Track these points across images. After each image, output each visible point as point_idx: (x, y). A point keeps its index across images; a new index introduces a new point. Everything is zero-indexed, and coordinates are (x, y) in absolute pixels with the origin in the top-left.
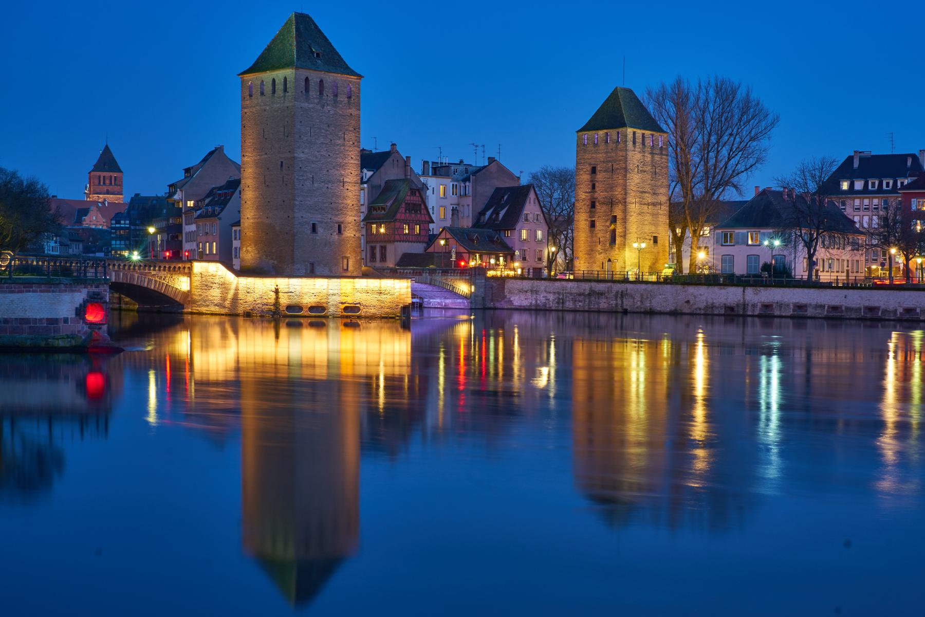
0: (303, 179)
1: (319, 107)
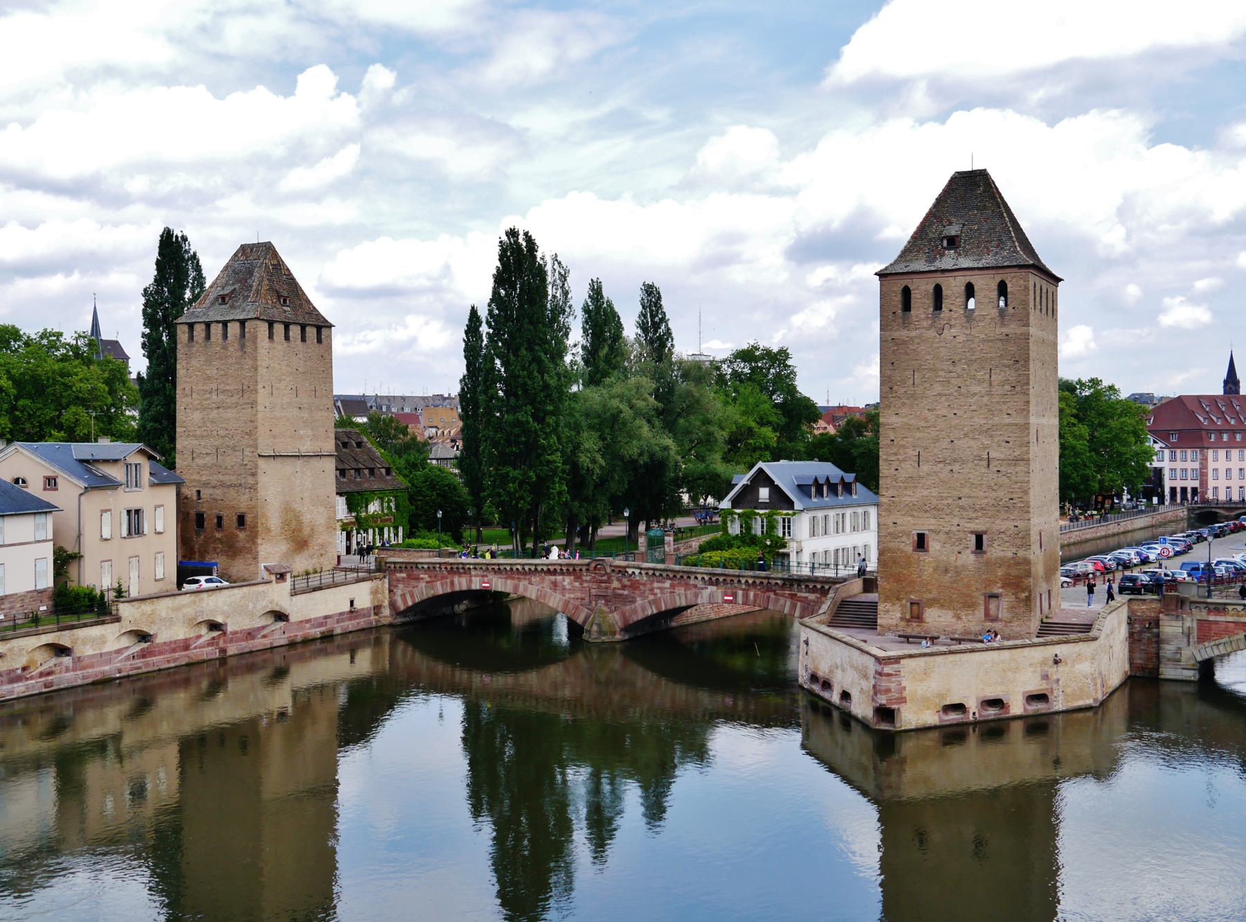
0: (898, 460)
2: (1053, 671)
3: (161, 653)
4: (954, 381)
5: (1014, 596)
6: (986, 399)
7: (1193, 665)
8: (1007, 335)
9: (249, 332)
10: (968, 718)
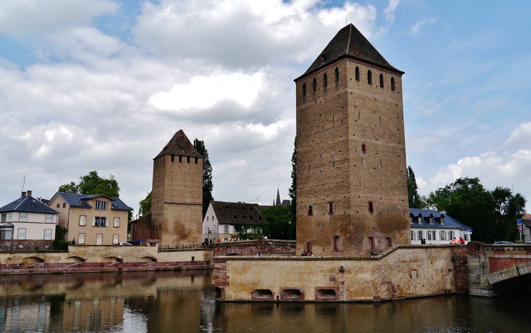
0: (302, 169)
1: (313, 103)
2: (340, 277)
3: (88, 266)
4: (321, 125)
5: (344, 237)
6: (332, 130)
7: (487, 286)
8: (339, 95)
10: (274, 299)
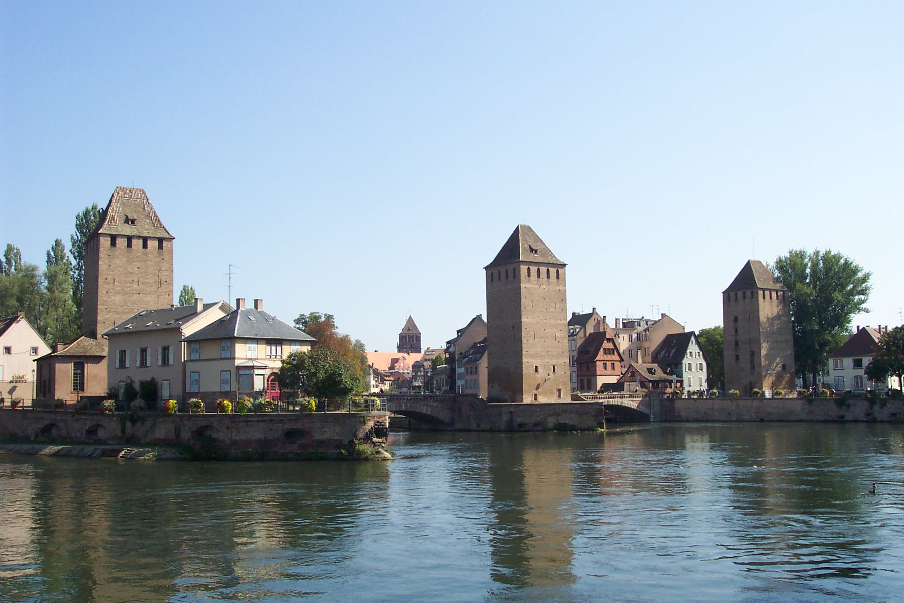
1: (537, 287)
9: (167, 246)
